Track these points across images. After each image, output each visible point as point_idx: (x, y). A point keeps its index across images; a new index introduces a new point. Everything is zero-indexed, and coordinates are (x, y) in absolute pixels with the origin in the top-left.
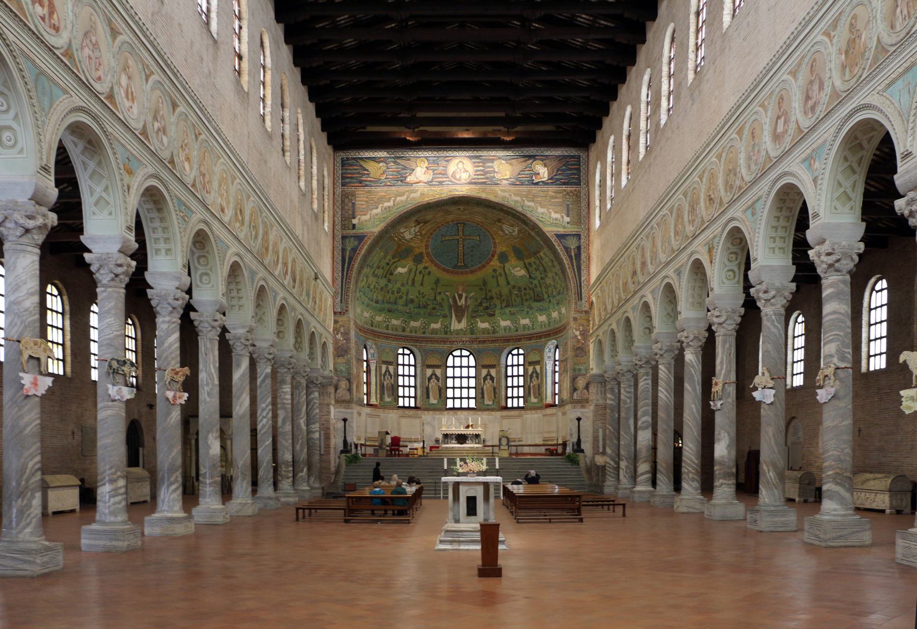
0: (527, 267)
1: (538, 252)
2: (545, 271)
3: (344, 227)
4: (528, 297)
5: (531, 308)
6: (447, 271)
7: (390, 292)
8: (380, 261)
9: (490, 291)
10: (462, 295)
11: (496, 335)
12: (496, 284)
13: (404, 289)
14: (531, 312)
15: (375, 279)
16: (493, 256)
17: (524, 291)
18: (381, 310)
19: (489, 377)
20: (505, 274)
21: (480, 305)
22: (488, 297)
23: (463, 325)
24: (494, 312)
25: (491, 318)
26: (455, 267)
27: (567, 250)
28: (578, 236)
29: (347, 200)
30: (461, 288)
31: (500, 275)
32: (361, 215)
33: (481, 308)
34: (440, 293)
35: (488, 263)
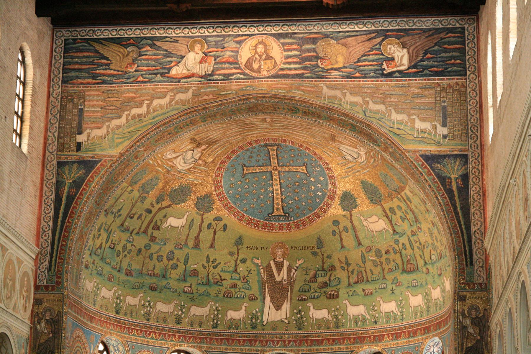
0: (387, 216)
1: (403, 189)
2: (417, 220)
4: (392, 265)
5: (398, 284)
6: (256, 225)
8: (133, 206)
9: (329, 257)
11: (342, 330)
12: (340, 245)
13: (180, 254)
15: (125, 236)
16: (332, 198)
17: (385, 256)
18: (136, 288)
20: (354, 228)
21: (314, 278)
22: (326, 267)
24: (338, 292)
25: (332, 302)
29: (70, 105)
31: (346, 229)
32: (92, 128)
33: (314, 285)
34: (244, 261)
35: (324, 211)
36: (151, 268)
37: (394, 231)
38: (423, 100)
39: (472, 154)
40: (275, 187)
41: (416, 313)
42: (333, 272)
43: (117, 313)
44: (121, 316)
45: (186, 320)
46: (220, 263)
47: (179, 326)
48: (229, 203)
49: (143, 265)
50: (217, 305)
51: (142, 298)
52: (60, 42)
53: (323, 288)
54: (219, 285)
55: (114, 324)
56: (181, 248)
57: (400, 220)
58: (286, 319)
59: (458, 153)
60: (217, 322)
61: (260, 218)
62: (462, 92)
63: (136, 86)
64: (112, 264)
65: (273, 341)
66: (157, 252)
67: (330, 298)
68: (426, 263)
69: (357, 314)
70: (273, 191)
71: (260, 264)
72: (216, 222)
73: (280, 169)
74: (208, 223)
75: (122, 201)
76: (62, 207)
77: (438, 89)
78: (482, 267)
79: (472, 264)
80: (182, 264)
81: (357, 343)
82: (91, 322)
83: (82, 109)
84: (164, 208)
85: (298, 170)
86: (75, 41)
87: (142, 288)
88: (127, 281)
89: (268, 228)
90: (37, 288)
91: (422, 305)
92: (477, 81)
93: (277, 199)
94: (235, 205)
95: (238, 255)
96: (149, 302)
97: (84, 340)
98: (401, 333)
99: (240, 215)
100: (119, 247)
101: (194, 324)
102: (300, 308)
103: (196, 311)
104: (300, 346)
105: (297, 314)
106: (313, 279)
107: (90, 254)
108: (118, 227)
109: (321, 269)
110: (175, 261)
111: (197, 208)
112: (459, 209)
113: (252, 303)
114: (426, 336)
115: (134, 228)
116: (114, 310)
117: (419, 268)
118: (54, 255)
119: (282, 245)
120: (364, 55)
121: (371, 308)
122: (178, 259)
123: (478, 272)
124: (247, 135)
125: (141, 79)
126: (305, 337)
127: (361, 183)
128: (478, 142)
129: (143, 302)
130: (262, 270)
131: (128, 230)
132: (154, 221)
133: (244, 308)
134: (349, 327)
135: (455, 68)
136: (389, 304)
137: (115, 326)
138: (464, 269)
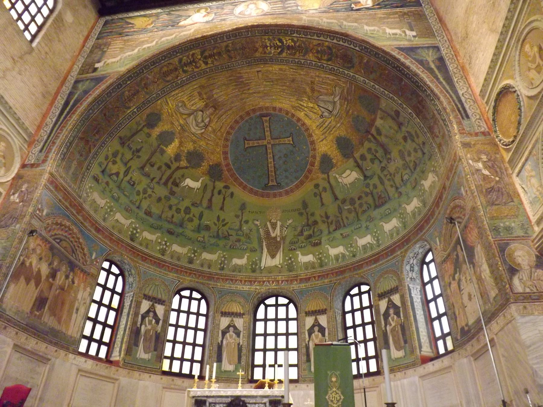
1: (374, 121)
2: (387, 152)
3: (82, 71)
6: (256, 193)
8: (153, 154)
9: (313, 214)
11: (325, 268)
12: (320, 204)
13: (195, 211)
14: (371, 225)
15: (145, 181)
16: (313, 165)
19: (316, 329)
20: (331, 187)
21: (301, 233)
23: (278, 260)
26: (266, 187)
27: (422, 63)
28: (437, 48)
31: (325, 189)
32: (108, 59)
33: (302, 238)
34: (247, 222)
35: (307, 177)
36: (170, 216)
37: (365, 177)
38: (389, 20)
39: (442, 45)
40: (269, 160)
41: (392, 235)
43: (132, 240)
45: (198, 262)
46: (228, 223)
50: (225, 254)
57: (370, 164)
58: (280, 264)
59: (430, 45)
62: (421, 17)
63: (151, 34)
64: (131, 198)
65: (269, 282)
66: (176, 205)
68: (397, 188)
74: (218, 190)
76: (68, 109)
77: (401, 14)
78: (480, 119)
79: (468, 117)
81: (339, 275)
83: (105, 51)
84: (182, 168)
85: (286, 142)
86: (112, 20)
90: (23, 166)
91: (397, 226)
92: (432, 8)
93: (271, 171)
94: (240, 175)
96: (166, 242)
97: (81, 240)
98: (379, 256)
100: (140, 188)
103: (206, 256)
105: (288, 260)
107: (103, 172)
108: (138, 168)
110: (191, 215)
111: (210, 176)
112: (441, 79)
114: (406, 247)
116: (129, 237)
118: (49, 141)
120: (335, 2)
123: (477, 123)
124: (245, 102)
125: (156, 30)
126: (295, 277)
127: (336, 141)
128: (445, 38)
129: (159, 241)
131: (149, 176)
133: (246, 257)
134: (332, 265)
135: (411, 4)
138: (461, 122)
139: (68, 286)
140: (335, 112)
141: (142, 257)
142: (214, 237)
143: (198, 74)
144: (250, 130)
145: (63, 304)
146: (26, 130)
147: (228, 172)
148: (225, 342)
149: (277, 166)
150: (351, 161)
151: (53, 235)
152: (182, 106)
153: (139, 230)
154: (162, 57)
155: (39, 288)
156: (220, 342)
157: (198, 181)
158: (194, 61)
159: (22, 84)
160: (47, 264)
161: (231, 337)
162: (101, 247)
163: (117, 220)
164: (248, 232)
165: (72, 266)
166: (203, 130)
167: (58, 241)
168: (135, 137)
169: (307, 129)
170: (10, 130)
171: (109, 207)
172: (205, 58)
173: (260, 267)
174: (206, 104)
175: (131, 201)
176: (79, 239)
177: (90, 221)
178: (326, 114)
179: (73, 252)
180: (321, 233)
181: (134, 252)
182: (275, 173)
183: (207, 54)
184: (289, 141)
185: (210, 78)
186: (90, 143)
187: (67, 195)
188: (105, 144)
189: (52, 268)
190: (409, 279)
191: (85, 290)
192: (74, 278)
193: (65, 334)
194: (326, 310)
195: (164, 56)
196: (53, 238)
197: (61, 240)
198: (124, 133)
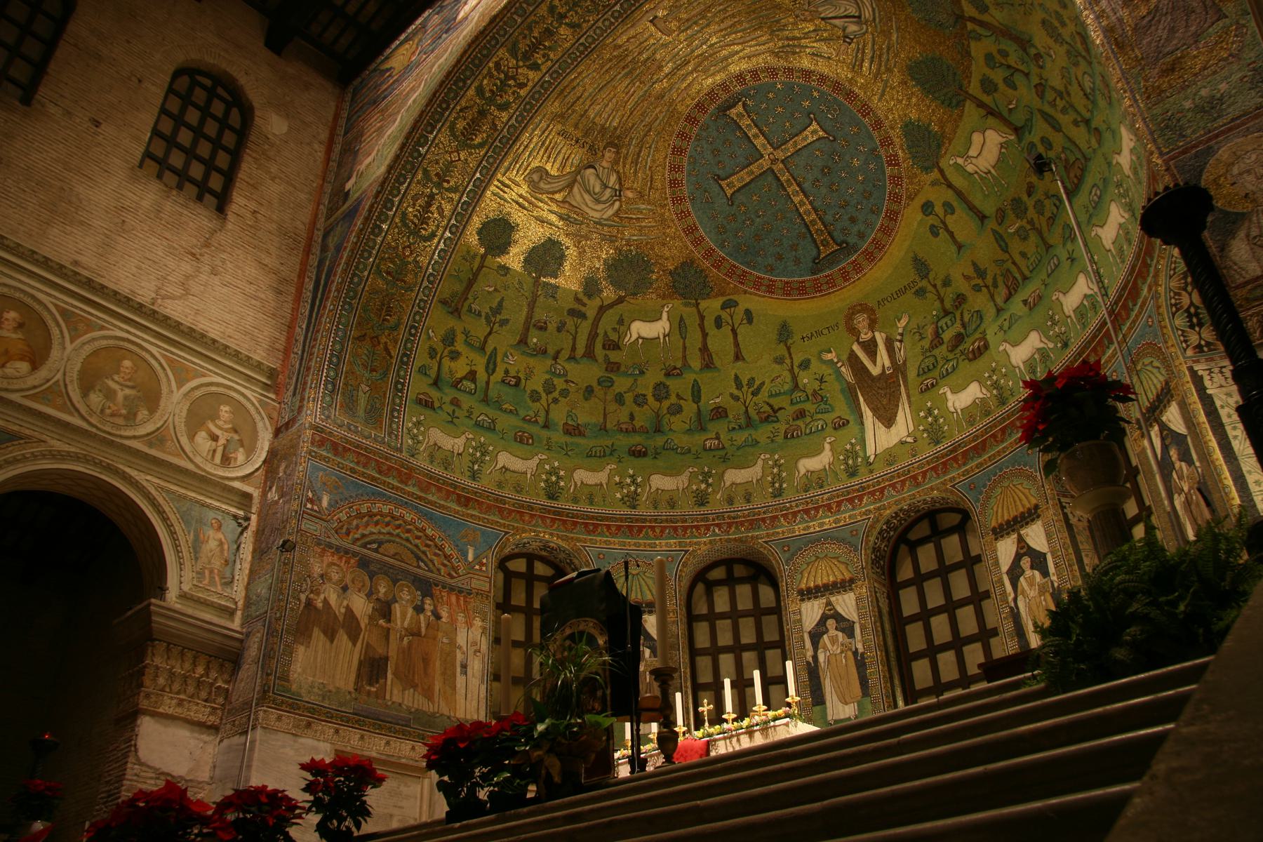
7: (629, 398)
8: (532, 306)
9: (947, 283)
10: (873, 340)
12: (954, 248)
19: (1026, 562)
20: (959, 194)
21: (937, 339)
22: (948, 305)
24: (984, 338)
25: (981, 363)
26: (817, 265)
30: (861, 321)
33: (942, 351)
34: (805, 365)
35: (896, 198)
37: (1017, 130)
40: (796, 200)
41: (1121, 251)
42: (963, 306)
43: (552, 497)
44: (561, 504)
45: (718, 497)
46: (763, 383)
47: (703, 508)
48: (734, 266)
49: (605, 416)
50: (776, 457)
51: (613, 472)
52: (348, 97)
53: (957, 346)
54: (773, 421)
55: (543, 518)
56: (678, 374)
60: (781, 486)
61: (801, 276)
64: (522, 413)
65: (893, 486)
67: (975, 358)
69: (1030, 355)
70: (797, 210)
71: (835, 360)
72: (728, 310)
73: (780, 155)
75: (492, 289)
80: (690, 402)
82: (466, 506)
84: (611, 306)
85: (810, 140)
86: (361, 83)
87: (611, 454)
88: (572, 443)
89: (825, 287)
90: (277, 432)
91: (1122, 220)
94: (748, 264)
95: (791, 358)
96: (631, 476)
97: (429, 532)
99: (766, 282)
101: (735, 500)
102: (929, 404)
103: (734, 476)
104: (945, 473)
105: (926, 417)
106: (936, 342)
107: (436, 383)
109: (942, 314)
110: (673, 399)
111: (681, 295)
113: (840, 432)
115: (556, 348)
117: (1088, 152)
119: (863, 308)
121: (1049, 323)
122: (678, 395)
126: (951, 451)
127: (913, 78)
129: (617, 479)
130: (843, 369)
131: (545, 352)
132: (601, 331)
133: (827, 446)
136: (1075, 287)
137: (548, 521)
139: (428, 626)
140: (867, 14)
141: (586, 525)
142: (740, 427)
143: (533, 97)
144: (717, 153)
145: (426, 661)
146: (258, 366)
147: (718, 267)
148: (821, 658)
149: (818, 204)
150: (969, 106)
151: (358, 539)
152: (541, 178)
153: (562, 473)
154: (440, 106)
155: (359, 644)
156: (811, 660)
157: (660, 319)
158: (508, 77)
159: (225, 290)
160: (362, 595)
161: (834, 641)
162: (483, 533)
163: (504, 467)
164: (816, 385)
165: (425, 587)
166: (617, 204)
167: (375, 546)
168: (475, 287)
169: (837, 86)
170: (229, 380)
171: (475, 449)
172: (526, 56)
173: (866, 458)
174: (591, 148)
175: (524, 419)
176: (423, 530)
177: (439, 489)
178: (853, 28)
179: (419, 558)
180: (981, 317)
181: (564, 522)
182: (823, 223)
183: (522, 47)
184: (814, 132)
185: (562, 91)
186: (383, 339)
187: (364, 455)
188: (416, 328)
189: (378, 599)
190: (1189, 353)
191: (469, 625)
192: (435, 607)
193: (449, 717)
194: (1036, 507)
195: (443, 101)
196: (359, 543)
197: (380, 543)
198: (447, 288)
